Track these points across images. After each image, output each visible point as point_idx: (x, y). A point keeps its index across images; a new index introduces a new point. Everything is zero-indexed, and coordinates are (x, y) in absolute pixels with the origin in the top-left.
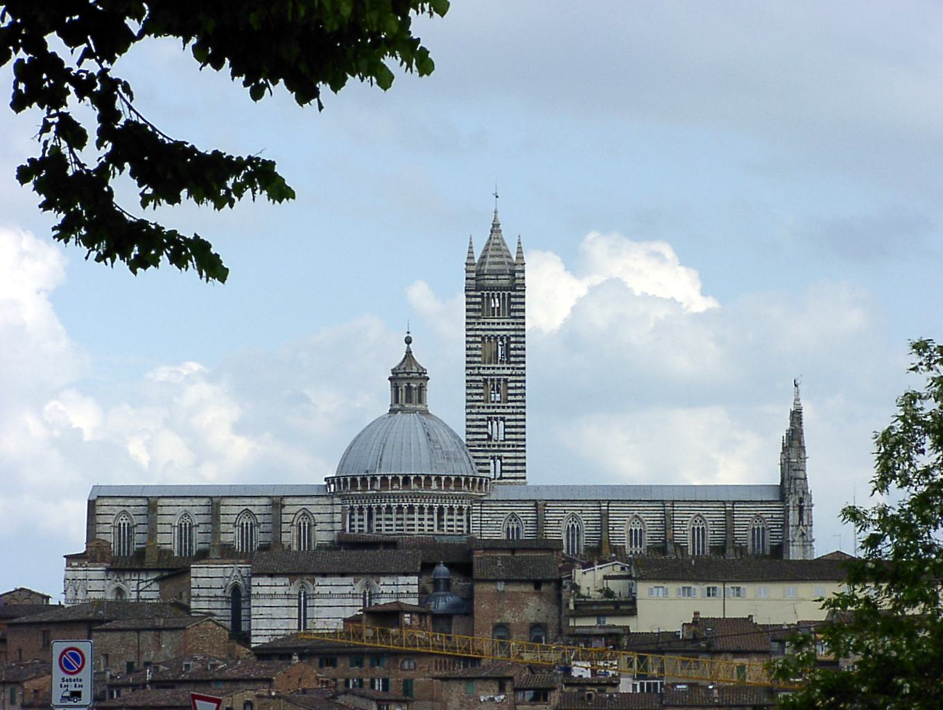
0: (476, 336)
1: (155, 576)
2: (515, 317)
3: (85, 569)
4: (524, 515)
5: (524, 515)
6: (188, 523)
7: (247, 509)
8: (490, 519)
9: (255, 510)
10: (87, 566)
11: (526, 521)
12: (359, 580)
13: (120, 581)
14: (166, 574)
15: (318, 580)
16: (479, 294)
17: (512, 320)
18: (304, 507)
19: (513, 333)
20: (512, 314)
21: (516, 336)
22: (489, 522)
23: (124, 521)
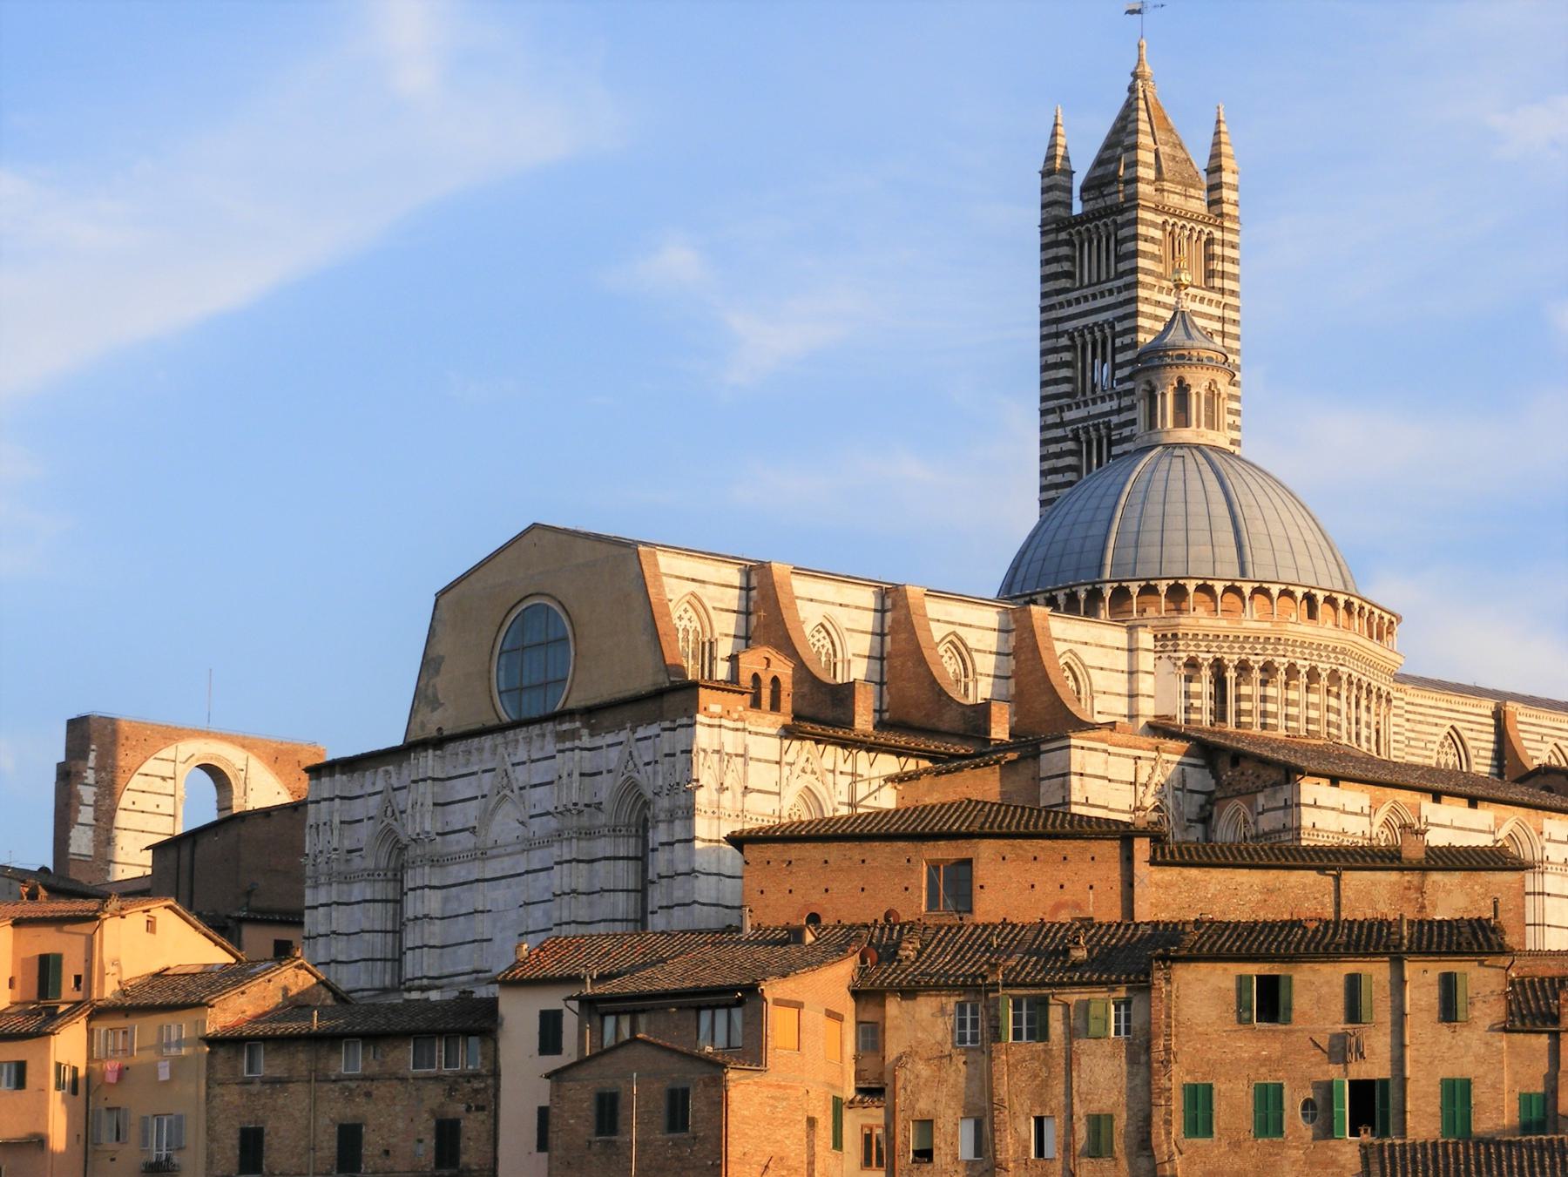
0: (1156, 318)
1: (889, 764)
2: (1222, 291)
3: (740, 725)
4: (1473, 735)
5: (1473, 735)
6: (824, 652)
7: (954, 633)
8: (1412, 735)
9: (972, 638)
10: (741, 719)
11: (1478, 749)
12: (1504, 820)
13: (813, 772)
14: (911, 765)
15: (1427, 807)
16: (1160, 220)
17: (1216, 296)
18: (1071, 646)
19: (1218, 326)
20: (1217, 282)
21: (1223, 334)
22: (1412, 743)
23: (685, 622)
